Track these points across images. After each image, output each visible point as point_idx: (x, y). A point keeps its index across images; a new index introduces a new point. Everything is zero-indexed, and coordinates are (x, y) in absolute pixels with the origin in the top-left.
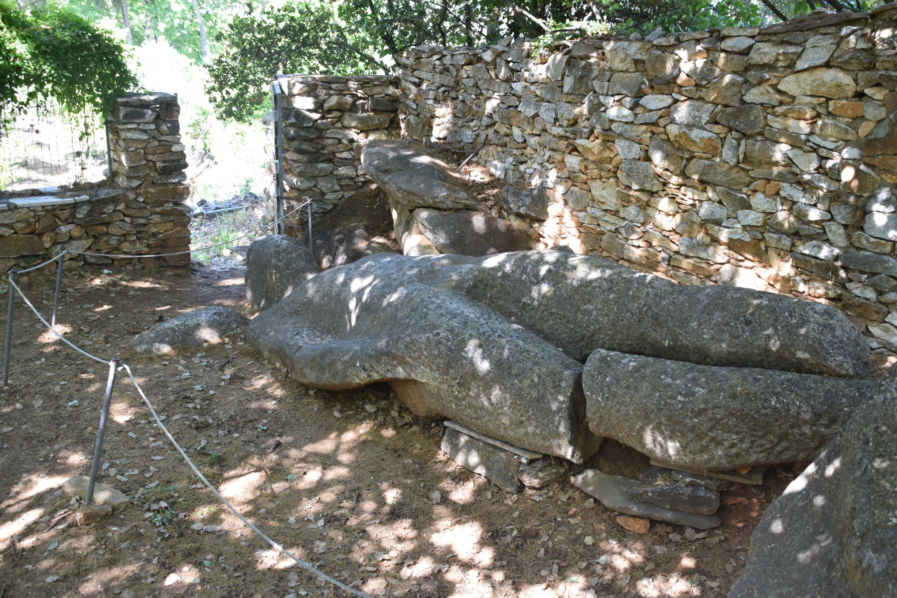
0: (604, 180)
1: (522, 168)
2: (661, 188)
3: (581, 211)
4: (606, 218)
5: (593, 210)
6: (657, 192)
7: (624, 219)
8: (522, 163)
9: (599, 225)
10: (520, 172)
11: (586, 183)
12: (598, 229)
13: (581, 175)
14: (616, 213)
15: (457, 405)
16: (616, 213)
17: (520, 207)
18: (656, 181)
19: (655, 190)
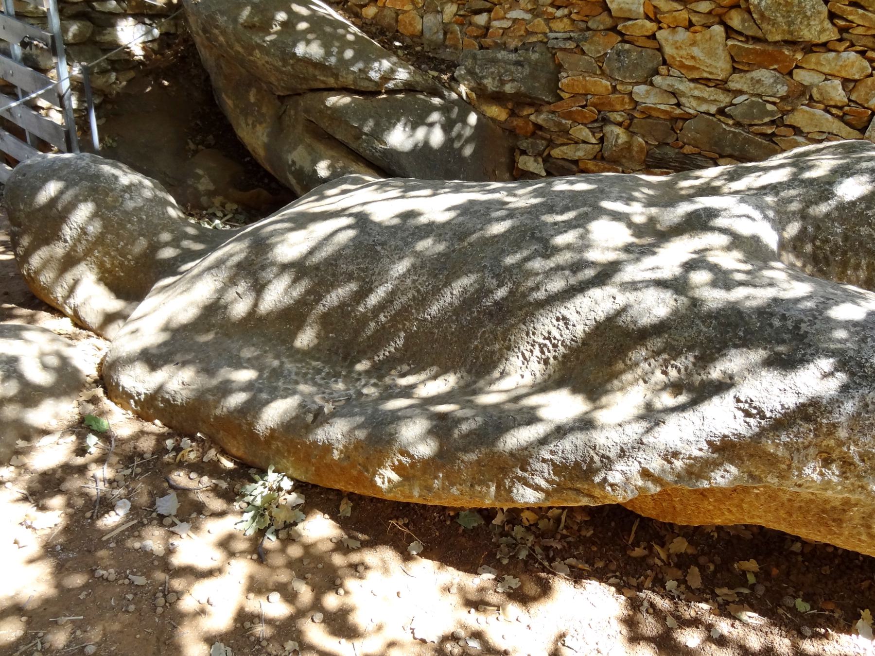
0: (698, 28)
1: (481, 19)
2: (838, 37)
3: (637, 84)
4: (696, 93)
5: (669, 81)
6: (825, 46)
7: (740, 92)
8: (478, 12)
9: (678, 105)
10: (478, 27)
11: (653, 37)
12: (678, 111)
13: (648, 24)
14: (721, 85)
16: (721, 85)
17: (502, 83)
18: (827, 25)
19: (824, 38)
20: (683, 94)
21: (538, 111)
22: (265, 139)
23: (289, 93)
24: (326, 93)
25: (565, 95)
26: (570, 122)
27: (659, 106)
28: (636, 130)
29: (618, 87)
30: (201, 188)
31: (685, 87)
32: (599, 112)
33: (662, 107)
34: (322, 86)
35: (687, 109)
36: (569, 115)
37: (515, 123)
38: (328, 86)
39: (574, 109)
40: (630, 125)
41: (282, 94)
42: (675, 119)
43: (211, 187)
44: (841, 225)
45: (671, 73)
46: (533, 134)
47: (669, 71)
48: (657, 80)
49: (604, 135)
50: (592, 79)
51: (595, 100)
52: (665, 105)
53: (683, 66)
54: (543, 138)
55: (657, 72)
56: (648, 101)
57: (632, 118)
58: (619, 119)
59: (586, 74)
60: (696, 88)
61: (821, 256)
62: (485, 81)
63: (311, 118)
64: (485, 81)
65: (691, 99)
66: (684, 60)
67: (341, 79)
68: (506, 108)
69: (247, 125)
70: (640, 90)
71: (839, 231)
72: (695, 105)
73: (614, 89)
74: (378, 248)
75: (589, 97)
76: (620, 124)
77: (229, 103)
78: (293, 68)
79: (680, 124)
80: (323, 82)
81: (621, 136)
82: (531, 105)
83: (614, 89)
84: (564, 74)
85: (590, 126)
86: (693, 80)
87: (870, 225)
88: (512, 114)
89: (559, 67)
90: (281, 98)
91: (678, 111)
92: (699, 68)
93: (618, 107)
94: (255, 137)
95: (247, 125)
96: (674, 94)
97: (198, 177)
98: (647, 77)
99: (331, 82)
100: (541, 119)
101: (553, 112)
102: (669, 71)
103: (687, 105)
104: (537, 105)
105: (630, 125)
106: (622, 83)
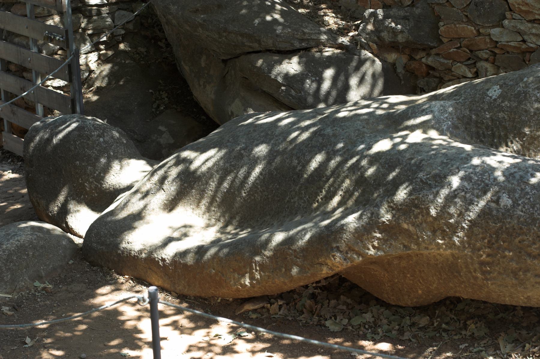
3: (493, 27)
4: (534, 31)
5: (513, 23)
9: (524, 41)
12: (524, 46)
15: (484, 273)
20: (525, 33)
21: (428, 55)
22: (213, 96)
23: (229, 57)
24: (253, 55)
25: (445, 40)
26: (451, 61)
27: (510, 44)
28: (499, 64)
29: (481, 31)
30: (162, 141)
31: (523, 27)
32: (471, 51)
33: (512, 44)
34: (251, 50)
35: (529, 44)
36: (448, 56)
37: (413, 66)
38: (255, 50)
39: (452, 50)
40: (494, 60)
41: (224, 58)
42: (523, 53)
43: (172, 141)
44: (489, 113)
45: (514, 17)
46: (428, 74)
47: (512, 15)
48: (506, 22)
49: (477, 69)
50: (461, 26)
51: (465, 42)
52: (514, 41)
53: (521, 11)
54: (435, 77)
55: (505, 18)
56: (502, 40)
57: (495, 54)
58: (485, 56)
59: (456, 23)
60: (533, 27)
61: (481, 132)
62: (383, 34)
63: (245, 76)
64: (383, 34)
65: (531, 36)
66: (521, 7)
67: (263, 43)
68: (405, 54)
69: (200, 85)
70: (496, 31)
71: (488, 116)
72: (534, 40)
73: (479, 34)
74: (242, 152)
75: (462, 40)
76: (487, 60)
77: (186, 68)
78: (226, 38)
79: (527, 55)
80: (250, 47)
81: (489, 69)
82: (424, 50)
83: (479, 34)
84: (441, 24)
85: (466, 63)
86: (530, 21)
87: (503, 111)
88: (411, 58)
89: (439, 18)
90: (225, 61)
91: (524, 46)
92: (532, 12)
93: (482, 46)
94: (205, 94)
95: (200, 85)
96: (519, 33)
97: (161, 133)
98: (500, 21)
99: (256, 46)
100: (430, 61)
101: (438, 54)
102: (512, 15)
103: (529, 41)
104: (427, 50)
105: (494, 60)
106: (483, 27)
